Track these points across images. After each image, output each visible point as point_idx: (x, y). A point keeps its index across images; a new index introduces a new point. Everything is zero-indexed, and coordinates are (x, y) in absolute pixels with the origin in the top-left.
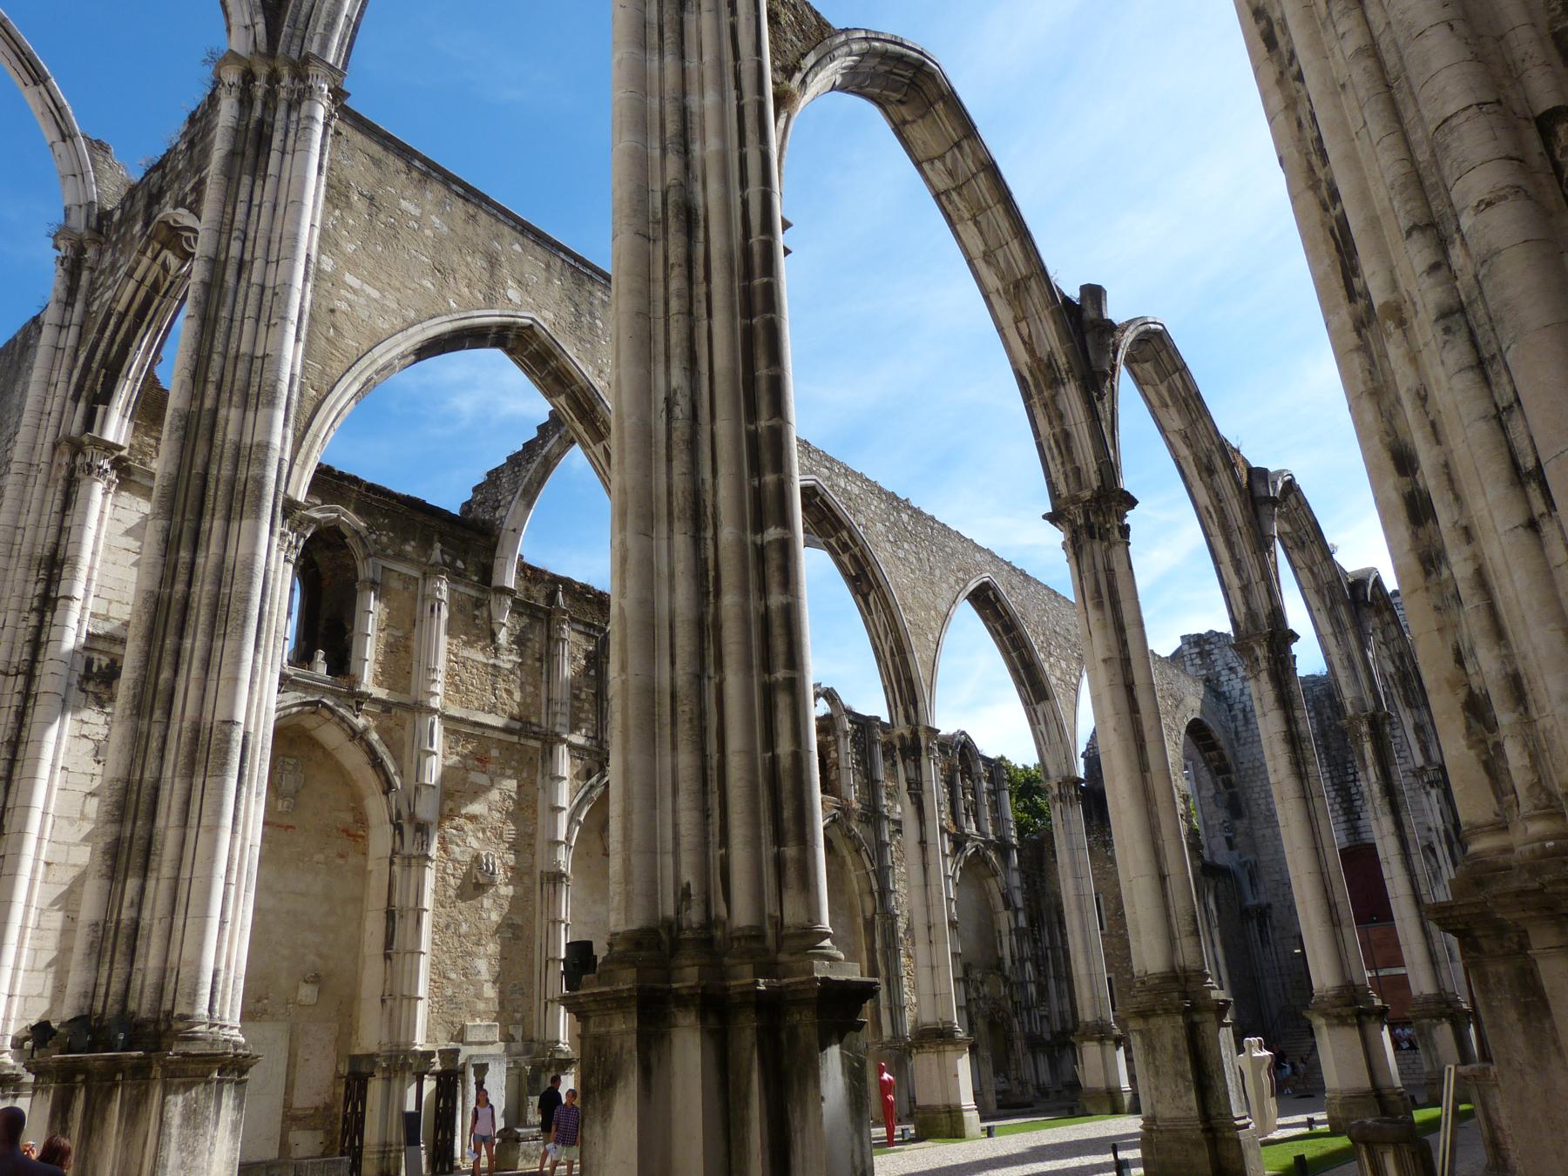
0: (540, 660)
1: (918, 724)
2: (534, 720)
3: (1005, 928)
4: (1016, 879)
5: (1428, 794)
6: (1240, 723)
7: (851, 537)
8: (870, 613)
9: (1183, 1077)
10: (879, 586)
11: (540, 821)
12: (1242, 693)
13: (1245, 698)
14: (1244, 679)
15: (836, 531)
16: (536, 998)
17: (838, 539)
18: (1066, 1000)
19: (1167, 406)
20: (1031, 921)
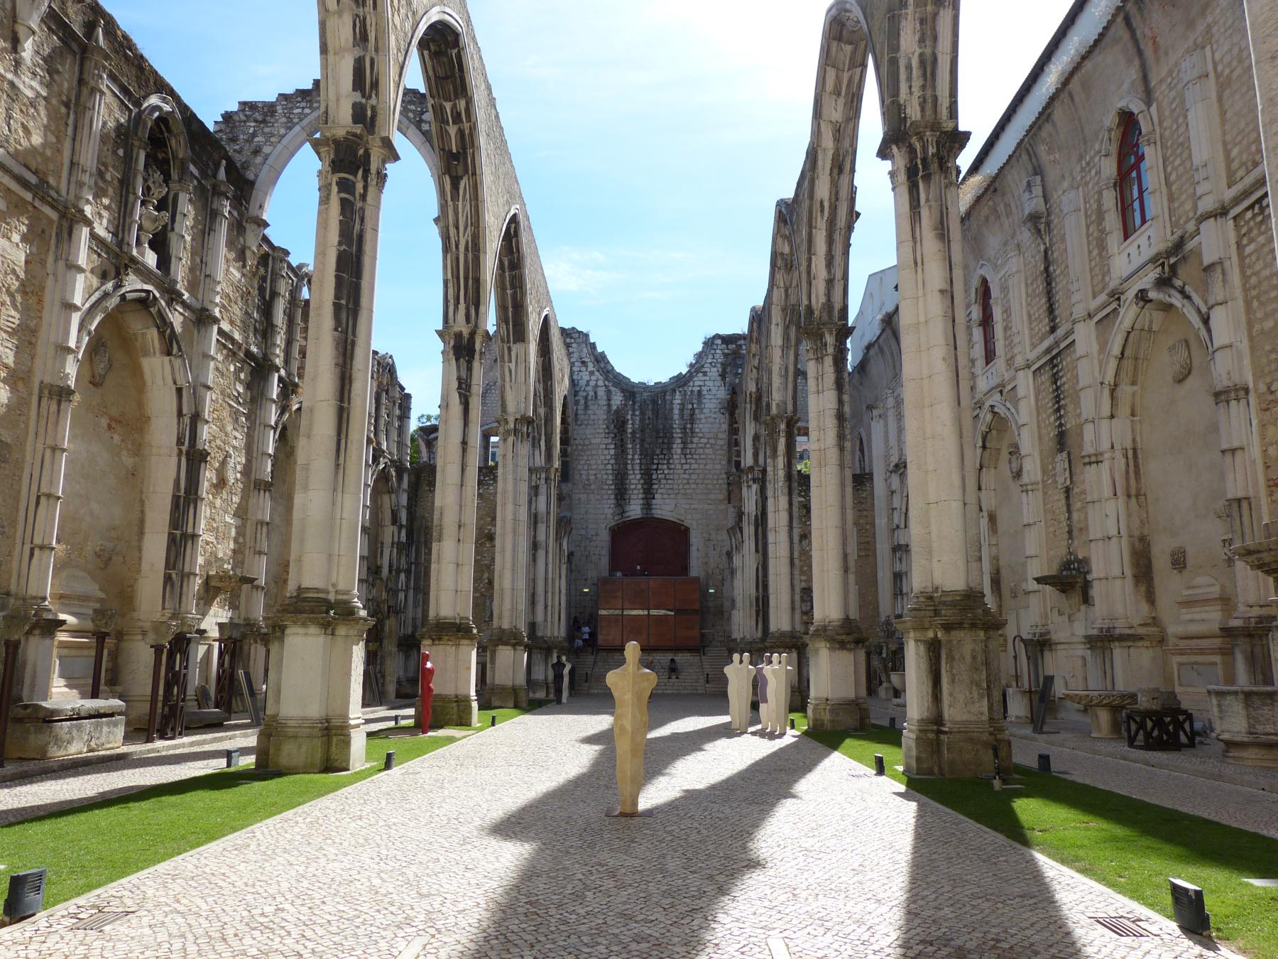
0: (67, 105)
1: (476, 326)
2: (52, 181)
3: (388, 540)
4: (404, 499)
5: (749, 487)
6: (581, 407)
7: (468, 110)
8: (455, 197)
9: (978, 685)
10: (474, 174)
11: (45, 315)
12: (588, 384)
13: (589, 388)
14: (592, 373)
15: (456, 97)
16: (19, 541)
17: (454, 106)
18: (420, 610)
19: (839, 94)
20: (410, 535)
